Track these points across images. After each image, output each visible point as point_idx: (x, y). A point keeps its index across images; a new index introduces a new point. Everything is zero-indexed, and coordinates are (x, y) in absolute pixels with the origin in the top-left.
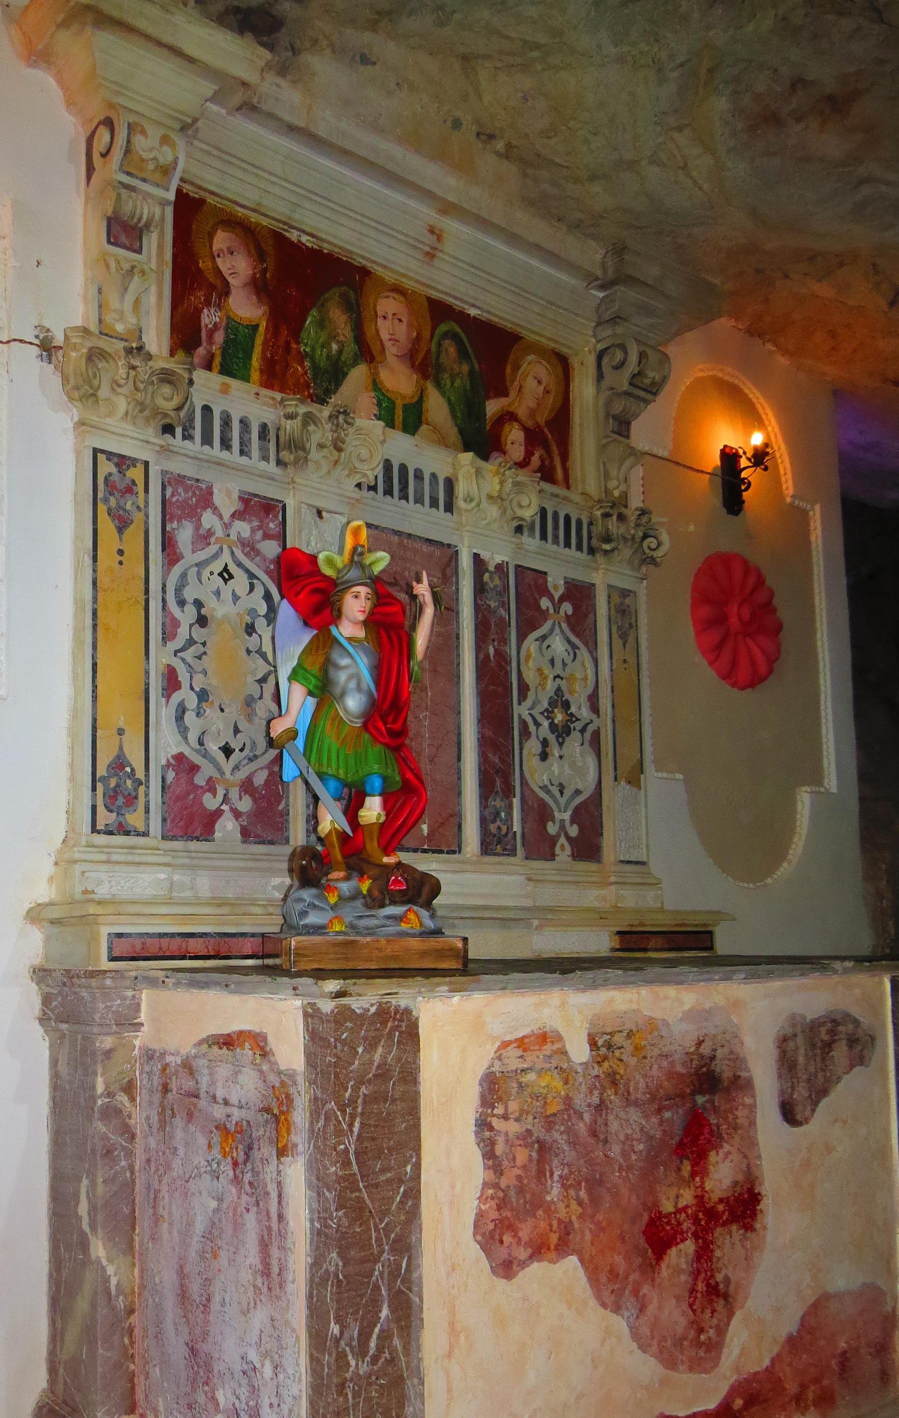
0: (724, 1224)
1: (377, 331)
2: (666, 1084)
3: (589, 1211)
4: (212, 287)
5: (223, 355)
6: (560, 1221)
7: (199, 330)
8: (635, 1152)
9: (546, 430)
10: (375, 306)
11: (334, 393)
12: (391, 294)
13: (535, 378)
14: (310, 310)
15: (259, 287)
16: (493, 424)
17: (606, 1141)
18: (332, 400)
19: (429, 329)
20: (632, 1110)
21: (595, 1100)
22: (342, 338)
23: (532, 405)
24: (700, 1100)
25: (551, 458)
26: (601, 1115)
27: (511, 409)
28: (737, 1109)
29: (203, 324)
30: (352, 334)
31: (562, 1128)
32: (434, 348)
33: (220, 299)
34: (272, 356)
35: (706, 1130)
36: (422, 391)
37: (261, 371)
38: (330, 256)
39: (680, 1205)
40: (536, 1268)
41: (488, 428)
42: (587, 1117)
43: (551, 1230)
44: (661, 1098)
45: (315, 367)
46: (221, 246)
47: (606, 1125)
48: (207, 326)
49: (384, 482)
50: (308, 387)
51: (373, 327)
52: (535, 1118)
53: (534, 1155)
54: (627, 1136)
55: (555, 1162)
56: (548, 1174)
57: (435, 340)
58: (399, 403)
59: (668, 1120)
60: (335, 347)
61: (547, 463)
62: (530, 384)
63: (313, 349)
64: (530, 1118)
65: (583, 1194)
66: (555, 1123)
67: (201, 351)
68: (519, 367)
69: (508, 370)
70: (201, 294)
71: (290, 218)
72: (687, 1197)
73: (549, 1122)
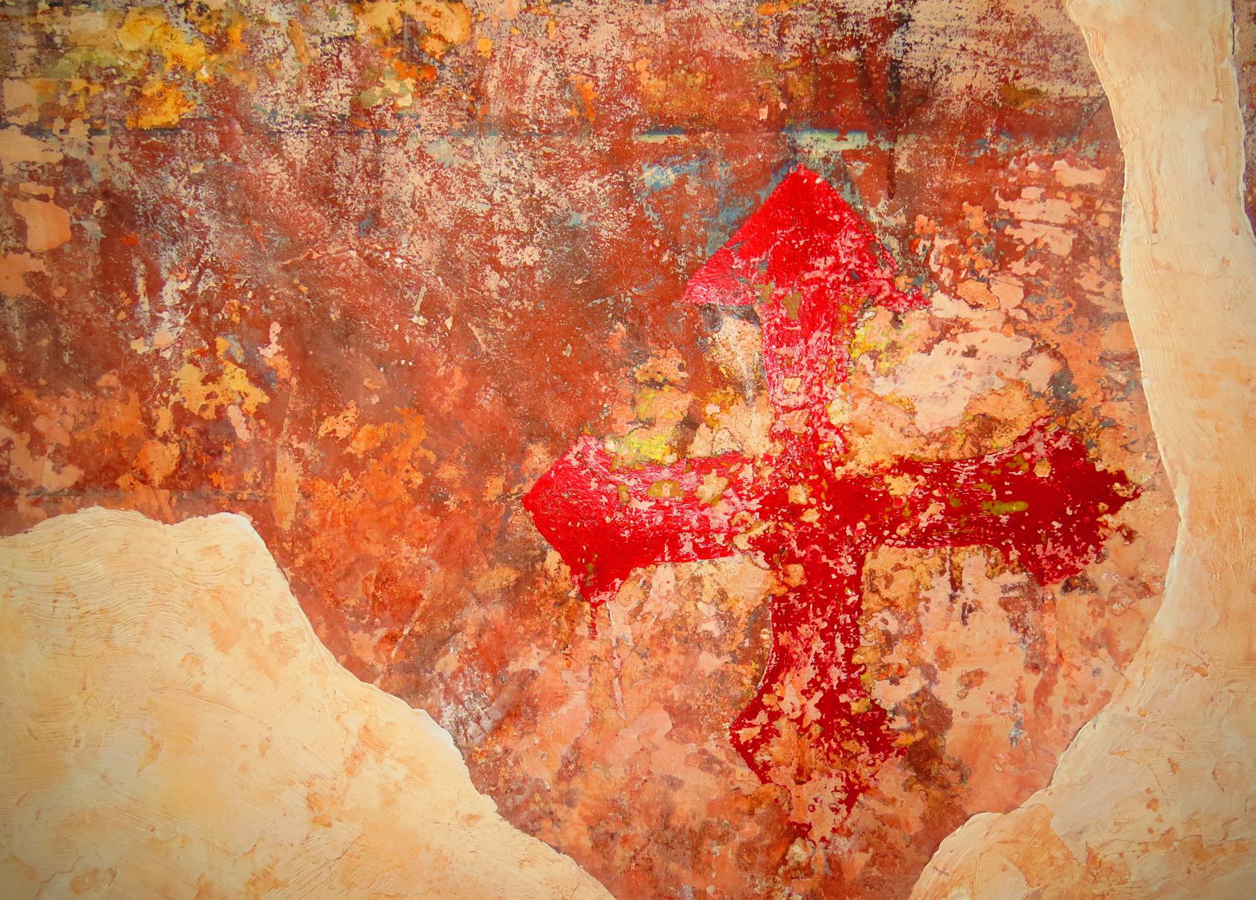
0: (921, 540)
2: (652, 84)
3: (295, 403)
6: (182, 416)
8: (498, 268)
17: (372, 220)
20: (490, 145)
21: (336, 98)
24: (819, 147)
26: (353, 149)
28: (1014, 195)
31: (197, 169)
35: (846, 242)
39: (700, 448)
40: (95, 520)
42: (298, 147)
43: (152, 433)
44: (629, 124)
47: (374, 174)
52: (95, 131)
53: (92, 228)
54: (466, 220)
55: (169, 256)
56: (141, 284)
59: (658, 195)
64: (79, 130)
65: (271, 353)
66: (170, 153)
72: (748, 429)
73: (151, 150)
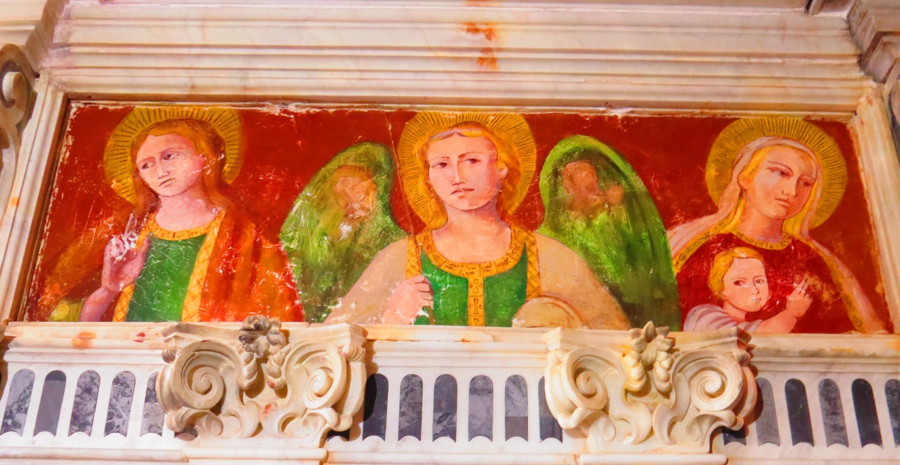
1: (429, 186)
4: (127, 207)
5: (137, 291)
7: (101, 267)
9: (814, 245)
10: (423, 154)
11: (343, 295)
12: (456, 130)
13: (773, 170)
14: (301, 189)
15: (208, 186)
16: (690, 264)
18: (339, 306)
19: (534, 156)
22: (360, 213)
23: (773, 210)
25: (836, 289)
27: (728, 229)
29: (107, 258)
30: (380, 203)
32: (544, 181)
33: (140, 219)
34: (227, 270)
36: (524, 252)
37: (204, 297)
38: (340, 114)
41: (676, 271)
45: (305, 267)
46: (151, 155)
48: (113, 259)
49: (402, 414)
50: (292, 296)
51: (421, 183)
57: (548, 168)
58: (477, 279)
60: (346, 229)
61: (826, 296)
62: (764, 181)
63: (303, 242)
67: (99, 295)
68: (734, 164)
69: (711, 172)
70: (109, 223)
71: (245, 88)
